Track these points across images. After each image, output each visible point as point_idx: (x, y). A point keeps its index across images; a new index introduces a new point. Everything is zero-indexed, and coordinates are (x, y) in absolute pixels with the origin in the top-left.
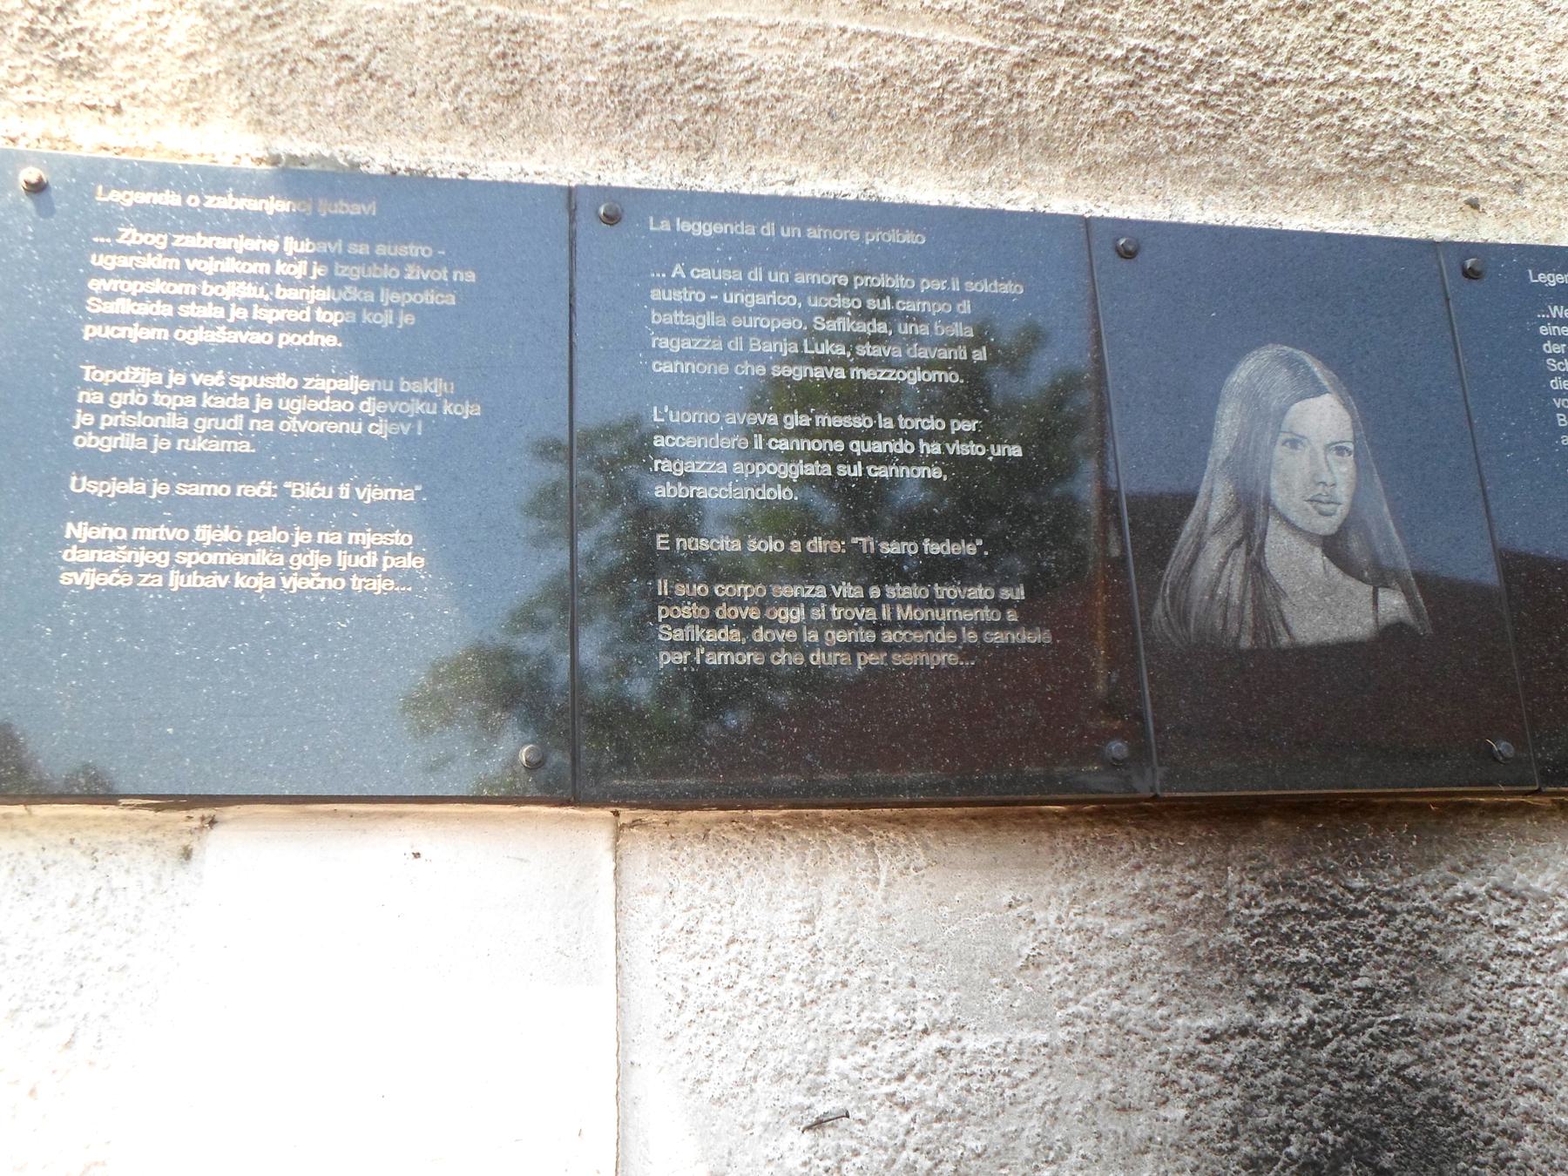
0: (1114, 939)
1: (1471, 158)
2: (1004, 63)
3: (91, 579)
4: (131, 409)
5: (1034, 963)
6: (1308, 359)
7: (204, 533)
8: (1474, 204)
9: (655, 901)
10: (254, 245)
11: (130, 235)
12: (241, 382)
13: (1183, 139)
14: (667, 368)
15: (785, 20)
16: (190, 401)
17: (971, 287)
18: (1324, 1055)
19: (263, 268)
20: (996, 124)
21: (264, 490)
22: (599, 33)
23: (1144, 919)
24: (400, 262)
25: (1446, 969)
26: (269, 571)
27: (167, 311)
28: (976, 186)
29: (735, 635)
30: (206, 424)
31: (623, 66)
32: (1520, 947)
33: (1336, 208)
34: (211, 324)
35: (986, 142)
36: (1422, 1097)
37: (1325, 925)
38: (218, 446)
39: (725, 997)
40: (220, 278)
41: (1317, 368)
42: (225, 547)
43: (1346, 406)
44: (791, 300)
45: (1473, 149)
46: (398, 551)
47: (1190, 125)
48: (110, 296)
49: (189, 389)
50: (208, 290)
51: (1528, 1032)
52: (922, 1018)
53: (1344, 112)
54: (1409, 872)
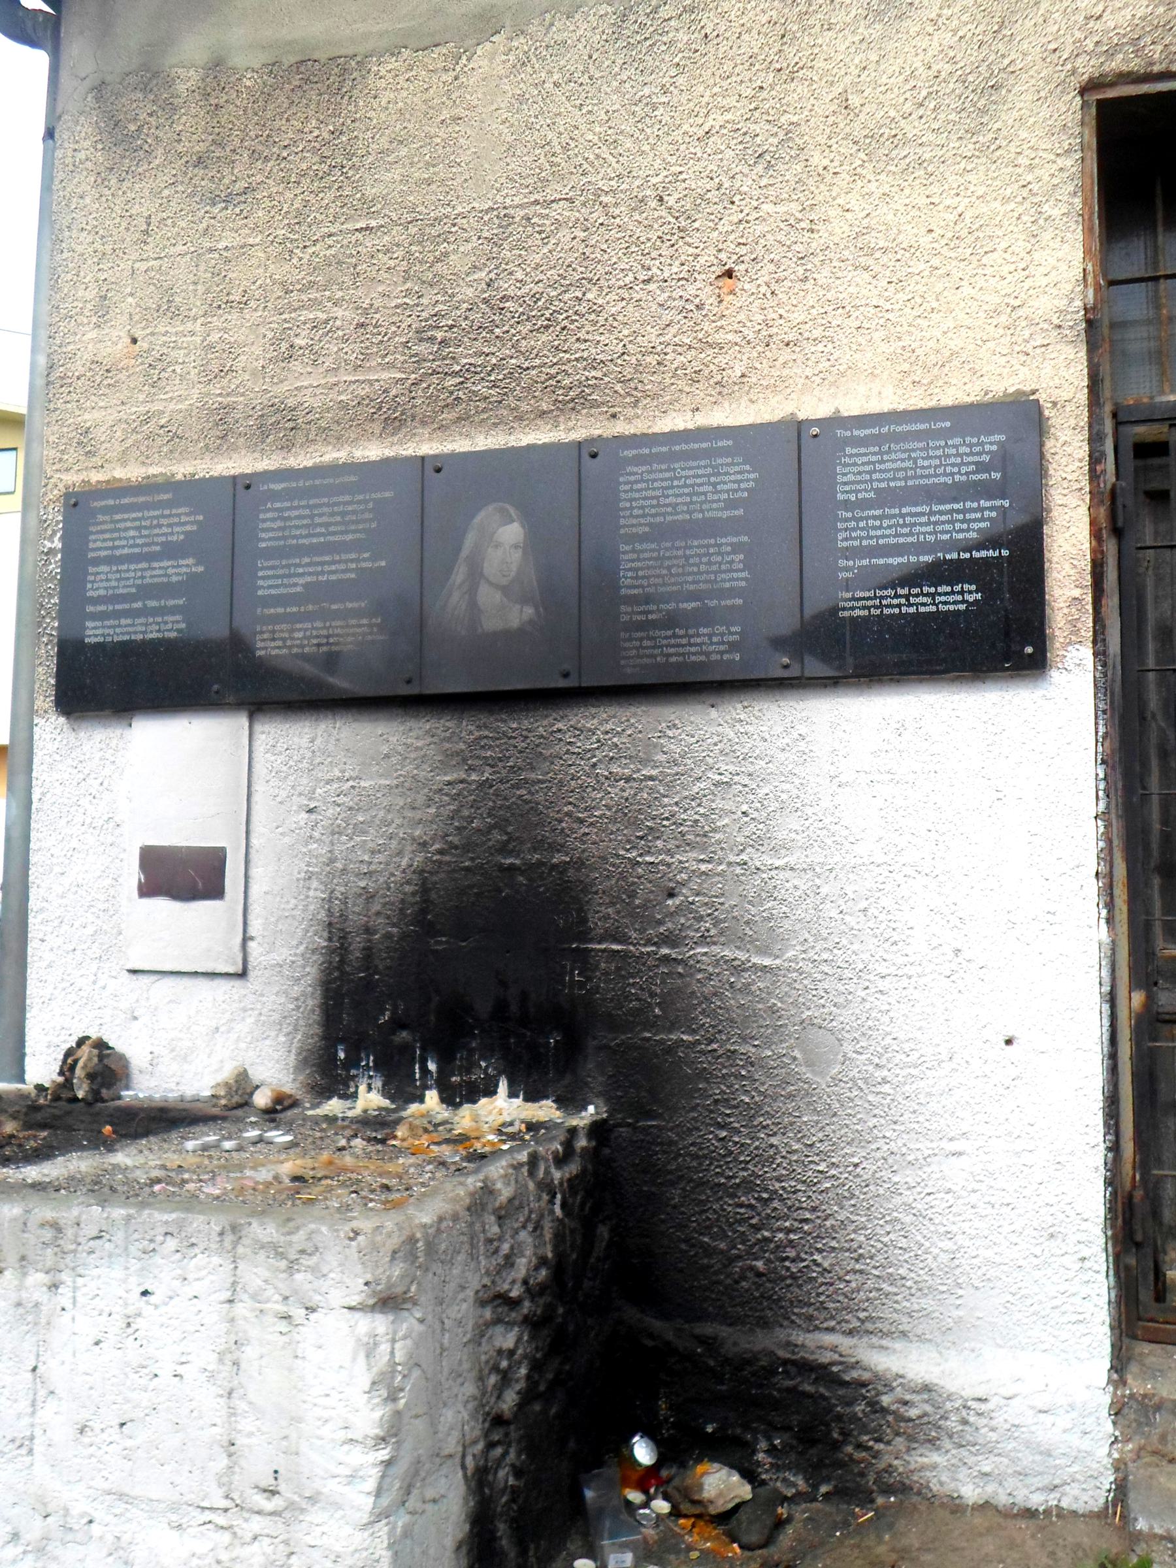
0: (417, 748)
1: (616, 392)
2: (408, 384)
3: (93, 640)
4: (102, 581)
5: (387, 756)
6: (508, 506)
7: (123, 621)
8: (614, 416)
9: (264, 736)
10: (134, 515)
11: (100, 518)
12: (132, 567)
13: (482, 405)
14: (264, 545)
15: (323, 382)
16: (118, 576)
17: (374, 496)
18: (491, 791)
19: (137, 523)
20: (402, 414)
21: (139, 605)
22: (255, 402)
23: (429, 740)
24: (179, 515)
25: (545, 759)
26: (141, 632)
27: (110, 544)
28: (393, 444)
29: (280, 643)
30: (123, 583)
31: (262, 416)
32: (576, 750)
33: (549, 426)
34: (123, 547)
35: (397, 424)
36: (527, 807)
37: (498, 742)
38: (125, 591)
39: (285, 768)
40: (126, 529)
41: (512, 511)
42: (129, 625)
43: (523, 527)
44: (307, 512)
45: (618, 387)
46: (178, 622)
47: (486, 398)
48: (95, 541)
49: (118, 571)
50: (123, 534)
51: (573, 783)
52: (347, 774)
53: (559, 377)
54: (537, 721)
